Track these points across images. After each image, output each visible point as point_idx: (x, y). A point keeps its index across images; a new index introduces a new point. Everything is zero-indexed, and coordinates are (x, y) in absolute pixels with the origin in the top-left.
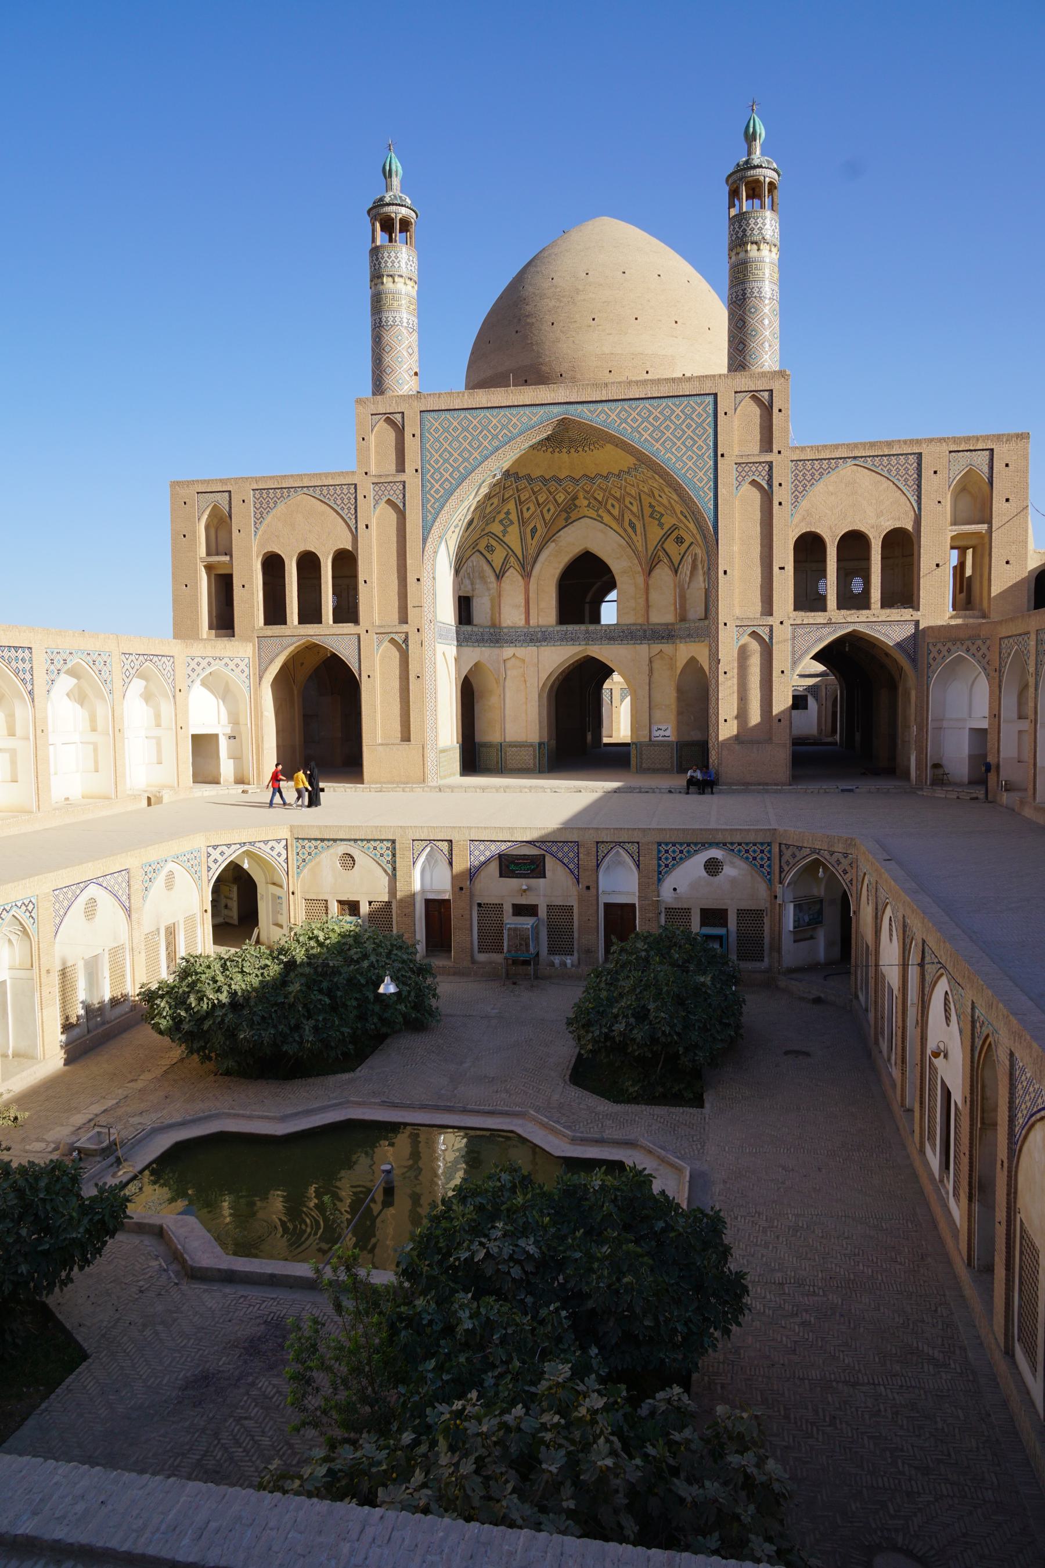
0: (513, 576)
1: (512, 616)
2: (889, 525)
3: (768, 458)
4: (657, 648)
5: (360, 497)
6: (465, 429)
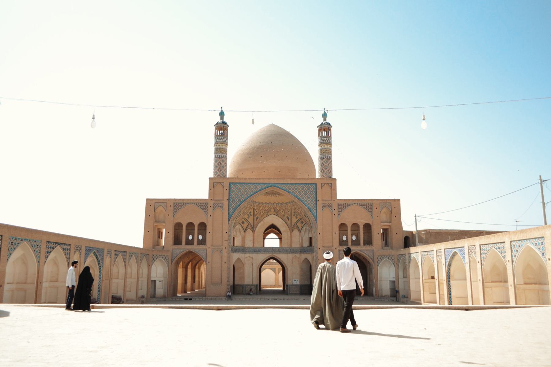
0: (249, 231)
1: (249, 244)
3: (330, 202)
4: (294, 255)
6: (243, 188)
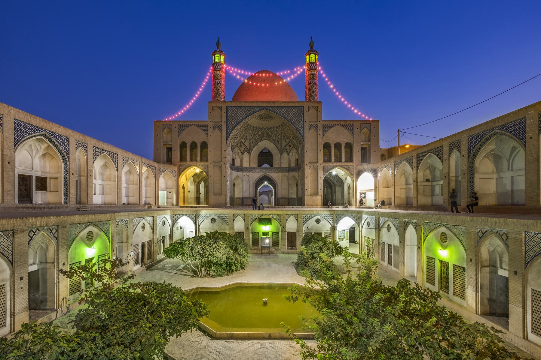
0: (246, 154)
1: (246, 164)
2: (346, 141)
4: (284, 173)
5: (209, 128)
